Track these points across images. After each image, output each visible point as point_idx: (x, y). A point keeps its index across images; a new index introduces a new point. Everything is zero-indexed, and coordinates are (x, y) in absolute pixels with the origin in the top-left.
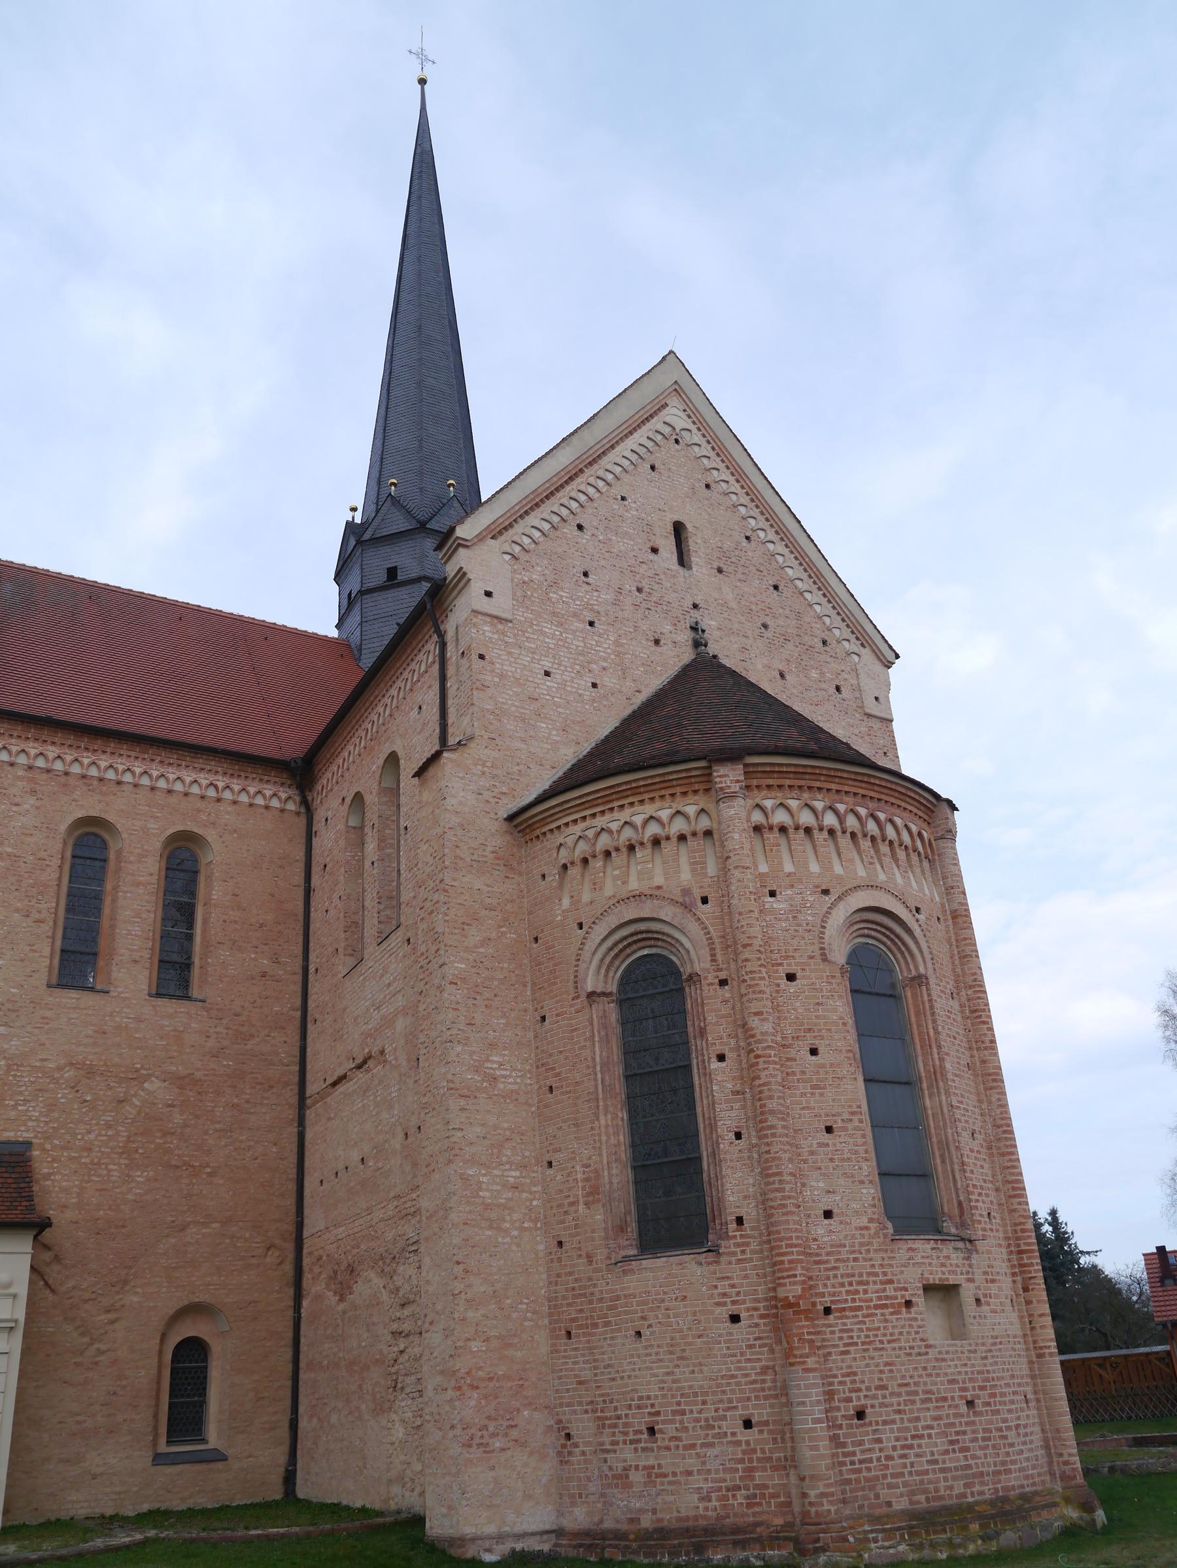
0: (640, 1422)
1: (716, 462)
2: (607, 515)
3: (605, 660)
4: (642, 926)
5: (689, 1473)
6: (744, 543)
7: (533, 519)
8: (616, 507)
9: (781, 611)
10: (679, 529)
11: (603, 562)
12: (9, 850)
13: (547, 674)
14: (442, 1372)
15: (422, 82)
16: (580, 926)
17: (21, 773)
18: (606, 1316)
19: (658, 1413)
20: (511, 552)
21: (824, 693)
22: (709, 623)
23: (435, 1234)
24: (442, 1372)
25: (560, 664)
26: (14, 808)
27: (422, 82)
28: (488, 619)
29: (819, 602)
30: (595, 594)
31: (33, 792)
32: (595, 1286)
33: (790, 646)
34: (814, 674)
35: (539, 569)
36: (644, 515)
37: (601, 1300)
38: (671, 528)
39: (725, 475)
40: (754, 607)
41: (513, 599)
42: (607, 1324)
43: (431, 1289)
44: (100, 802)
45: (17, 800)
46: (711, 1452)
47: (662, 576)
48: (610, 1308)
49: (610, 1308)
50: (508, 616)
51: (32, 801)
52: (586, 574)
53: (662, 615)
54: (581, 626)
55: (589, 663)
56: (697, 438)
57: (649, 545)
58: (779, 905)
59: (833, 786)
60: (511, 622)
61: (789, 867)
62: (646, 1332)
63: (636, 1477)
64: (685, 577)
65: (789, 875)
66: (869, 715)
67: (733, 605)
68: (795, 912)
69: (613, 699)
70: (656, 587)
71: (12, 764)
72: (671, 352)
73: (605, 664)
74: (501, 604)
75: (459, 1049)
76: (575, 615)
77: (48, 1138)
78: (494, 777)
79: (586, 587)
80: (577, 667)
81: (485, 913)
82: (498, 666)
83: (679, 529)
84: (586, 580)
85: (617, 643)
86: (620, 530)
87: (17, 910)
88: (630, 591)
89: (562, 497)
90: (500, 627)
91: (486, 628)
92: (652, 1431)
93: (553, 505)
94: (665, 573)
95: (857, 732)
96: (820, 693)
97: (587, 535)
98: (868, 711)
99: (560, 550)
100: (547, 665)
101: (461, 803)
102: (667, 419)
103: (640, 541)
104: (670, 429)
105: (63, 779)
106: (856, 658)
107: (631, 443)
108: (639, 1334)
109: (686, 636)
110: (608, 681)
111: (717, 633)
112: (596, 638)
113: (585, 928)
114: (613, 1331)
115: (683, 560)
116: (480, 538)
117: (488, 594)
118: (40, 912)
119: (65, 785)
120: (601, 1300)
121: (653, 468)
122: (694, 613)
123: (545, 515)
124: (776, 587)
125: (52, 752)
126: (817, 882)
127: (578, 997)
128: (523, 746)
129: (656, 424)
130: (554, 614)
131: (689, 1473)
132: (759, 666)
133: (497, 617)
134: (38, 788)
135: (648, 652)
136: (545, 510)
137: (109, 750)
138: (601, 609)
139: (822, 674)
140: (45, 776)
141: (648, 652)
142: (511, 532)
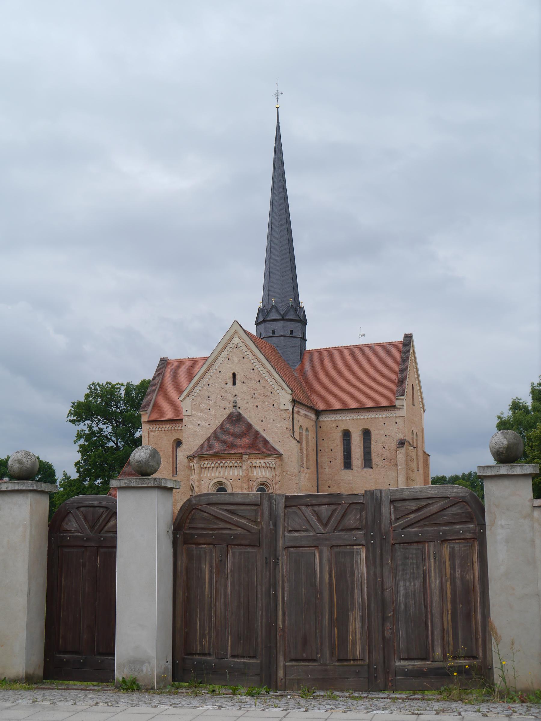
1: (246, 350)
2: (215, 379)
3: (212, 417)
6: (252, 371)
7: (197, 388)
8: (218, 375)
9: (259, 388)
10: (234, 375)
11: (213, 392)
12: (163, 449)
13: (199, 425)
15: (278, 108)
17: (163, 432)
20: (192, 398)
21: (269, 408)
22: (238, 399)
25: (201, 422)
26: (163, 440)
27: (278, 108)
28: (187, 416)
29: (271, 381)
30: (211, 401)
31: (166, 436)
33: (261, 397)
34: (267, 403)
35: (198, 400)
36: (225, 375)
38: (231, 375)
39: (249, 353)
40: (251, 390)
41: (192, 410)
44: (178, 435)
45: (163, 438)
47: (227, 390)
50: (191, 415)
51: (166, 438)
52: (209, 397)
53: (226, 401)
54: (206, 411)
55: (208, 419)
56: (241, 344)
57: (225, 383)
58: (203, 482)
59: (213, 458)
60: (191, 415)
61: (205, 476)
64: (234, 388)
65: (205, 477)
66: (281, 410)
67: (246, 391)
68: (205, 484)
69: (213, 427)
70: (226, 394)
71: (161, 431)
72: (235, 321)
73: (211, 419)
74: (189, 413)
75: (179, 504)
76: (206, 409)
77: (175, 506)
78: (187, 451)
79: (209, 400)
80: (205, 421)
81: (184, 479)
82: (188, 426)
83: (234, 375)
84: (208, 399)
85: (215, 412)
86: (218, 381)
87: (166, 462)
88: (219, 398)
89: (204, 379)
90: (189, 417)
91: (186, 419)
93: (202, 382)
94: (228, 389)
95: (277, 416)
96: (267, 408)
97: (210, 386)
98: (280, 409)
99: (203, 393)
100: (199, 423)
101: (180, 458)
102: (233, 343)
103: (223, 383)
104: (234, 345)
105: (170, 431)
106: (280, 394)
107: (223, 355)
109: (232, 405)
110: (212, 423)
111: (240, 401)
112: (210, 413)
115: (234, 384)
116: (185, 398)
117: (187, 411)
118: (169, 461)
119: (171, 433)
121: (229, 359)
122: (235, 398)
123: (200, 386)
124: (259, 381)
125: (168, 426)
126: (209, 478)
128: (193, 443)
129: (231, 345)
130: (201, 410)
132: (251, 406)
133: (188, 415)
134: (166, 434)
135: (222, 412)
136: (200, 385)
137: (178, 423)
138: (212, 405)
139: (269, 402)
140: (167, 432)
141: (222, 412)
142: (192, 393)
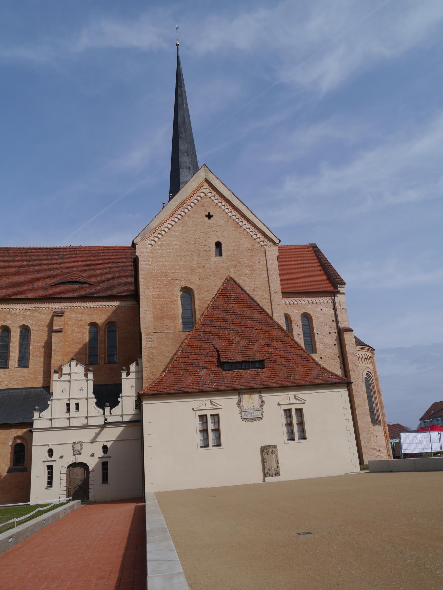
0: (378, 449)
4: (369, 373)
5: (383, 456)
14: (367, 440)
16: (362, 369)
18: (372, 433)
19: (380, 448)
23: (362, 417)
24: (367, 440)
32: (370, 429)
37: (371, 431)
42: (373, 434)
43: (361, 427)
46: (384, 453)
48: (373, 432)
49: (373, 432)
62: (377, 436)
63: (379, 457)
92: (379, 450)
108: (377, 436)
113: (363, 370)
114: (373, 436)
120: (371, 431)
127: (363, 382)
131: (383, 456)
